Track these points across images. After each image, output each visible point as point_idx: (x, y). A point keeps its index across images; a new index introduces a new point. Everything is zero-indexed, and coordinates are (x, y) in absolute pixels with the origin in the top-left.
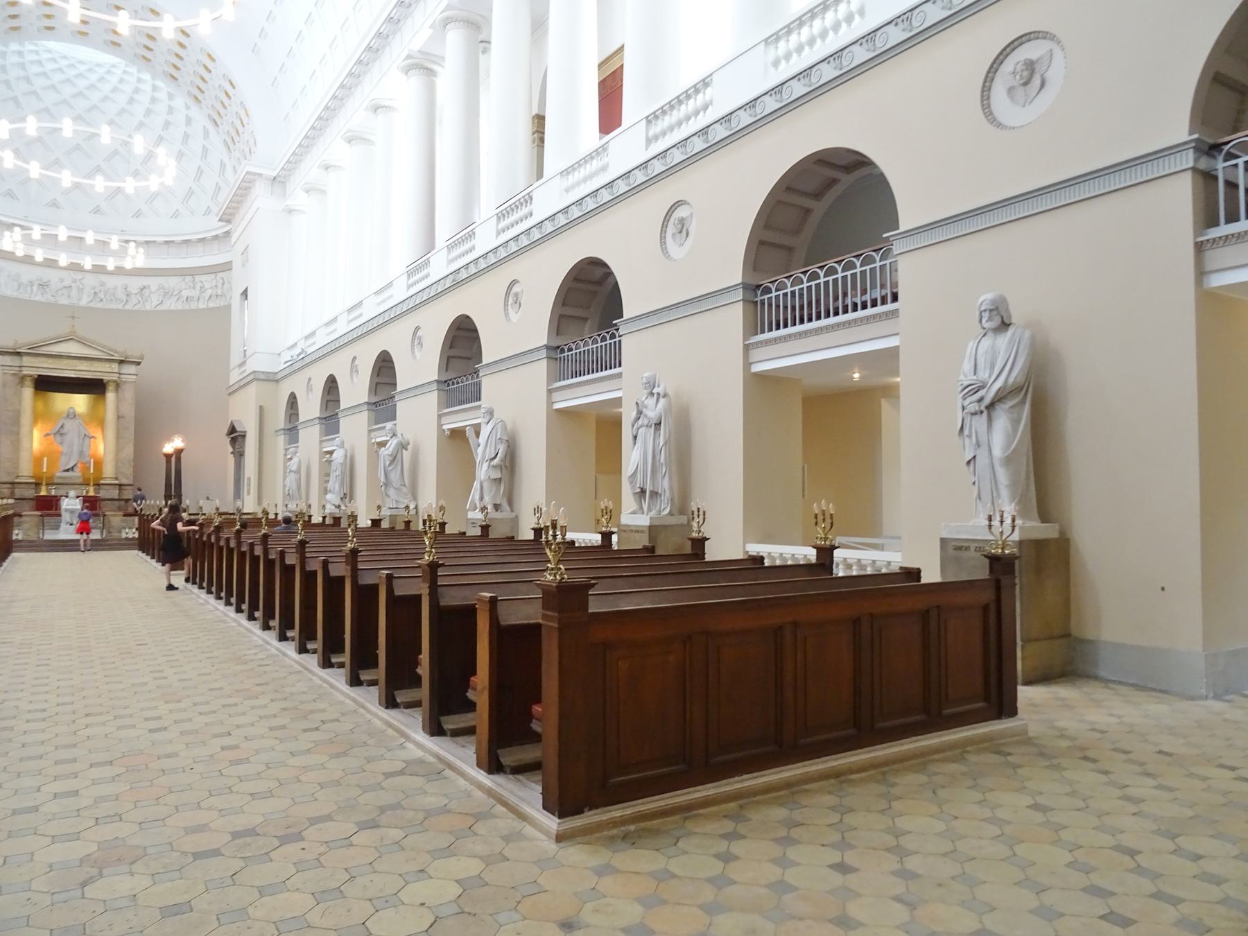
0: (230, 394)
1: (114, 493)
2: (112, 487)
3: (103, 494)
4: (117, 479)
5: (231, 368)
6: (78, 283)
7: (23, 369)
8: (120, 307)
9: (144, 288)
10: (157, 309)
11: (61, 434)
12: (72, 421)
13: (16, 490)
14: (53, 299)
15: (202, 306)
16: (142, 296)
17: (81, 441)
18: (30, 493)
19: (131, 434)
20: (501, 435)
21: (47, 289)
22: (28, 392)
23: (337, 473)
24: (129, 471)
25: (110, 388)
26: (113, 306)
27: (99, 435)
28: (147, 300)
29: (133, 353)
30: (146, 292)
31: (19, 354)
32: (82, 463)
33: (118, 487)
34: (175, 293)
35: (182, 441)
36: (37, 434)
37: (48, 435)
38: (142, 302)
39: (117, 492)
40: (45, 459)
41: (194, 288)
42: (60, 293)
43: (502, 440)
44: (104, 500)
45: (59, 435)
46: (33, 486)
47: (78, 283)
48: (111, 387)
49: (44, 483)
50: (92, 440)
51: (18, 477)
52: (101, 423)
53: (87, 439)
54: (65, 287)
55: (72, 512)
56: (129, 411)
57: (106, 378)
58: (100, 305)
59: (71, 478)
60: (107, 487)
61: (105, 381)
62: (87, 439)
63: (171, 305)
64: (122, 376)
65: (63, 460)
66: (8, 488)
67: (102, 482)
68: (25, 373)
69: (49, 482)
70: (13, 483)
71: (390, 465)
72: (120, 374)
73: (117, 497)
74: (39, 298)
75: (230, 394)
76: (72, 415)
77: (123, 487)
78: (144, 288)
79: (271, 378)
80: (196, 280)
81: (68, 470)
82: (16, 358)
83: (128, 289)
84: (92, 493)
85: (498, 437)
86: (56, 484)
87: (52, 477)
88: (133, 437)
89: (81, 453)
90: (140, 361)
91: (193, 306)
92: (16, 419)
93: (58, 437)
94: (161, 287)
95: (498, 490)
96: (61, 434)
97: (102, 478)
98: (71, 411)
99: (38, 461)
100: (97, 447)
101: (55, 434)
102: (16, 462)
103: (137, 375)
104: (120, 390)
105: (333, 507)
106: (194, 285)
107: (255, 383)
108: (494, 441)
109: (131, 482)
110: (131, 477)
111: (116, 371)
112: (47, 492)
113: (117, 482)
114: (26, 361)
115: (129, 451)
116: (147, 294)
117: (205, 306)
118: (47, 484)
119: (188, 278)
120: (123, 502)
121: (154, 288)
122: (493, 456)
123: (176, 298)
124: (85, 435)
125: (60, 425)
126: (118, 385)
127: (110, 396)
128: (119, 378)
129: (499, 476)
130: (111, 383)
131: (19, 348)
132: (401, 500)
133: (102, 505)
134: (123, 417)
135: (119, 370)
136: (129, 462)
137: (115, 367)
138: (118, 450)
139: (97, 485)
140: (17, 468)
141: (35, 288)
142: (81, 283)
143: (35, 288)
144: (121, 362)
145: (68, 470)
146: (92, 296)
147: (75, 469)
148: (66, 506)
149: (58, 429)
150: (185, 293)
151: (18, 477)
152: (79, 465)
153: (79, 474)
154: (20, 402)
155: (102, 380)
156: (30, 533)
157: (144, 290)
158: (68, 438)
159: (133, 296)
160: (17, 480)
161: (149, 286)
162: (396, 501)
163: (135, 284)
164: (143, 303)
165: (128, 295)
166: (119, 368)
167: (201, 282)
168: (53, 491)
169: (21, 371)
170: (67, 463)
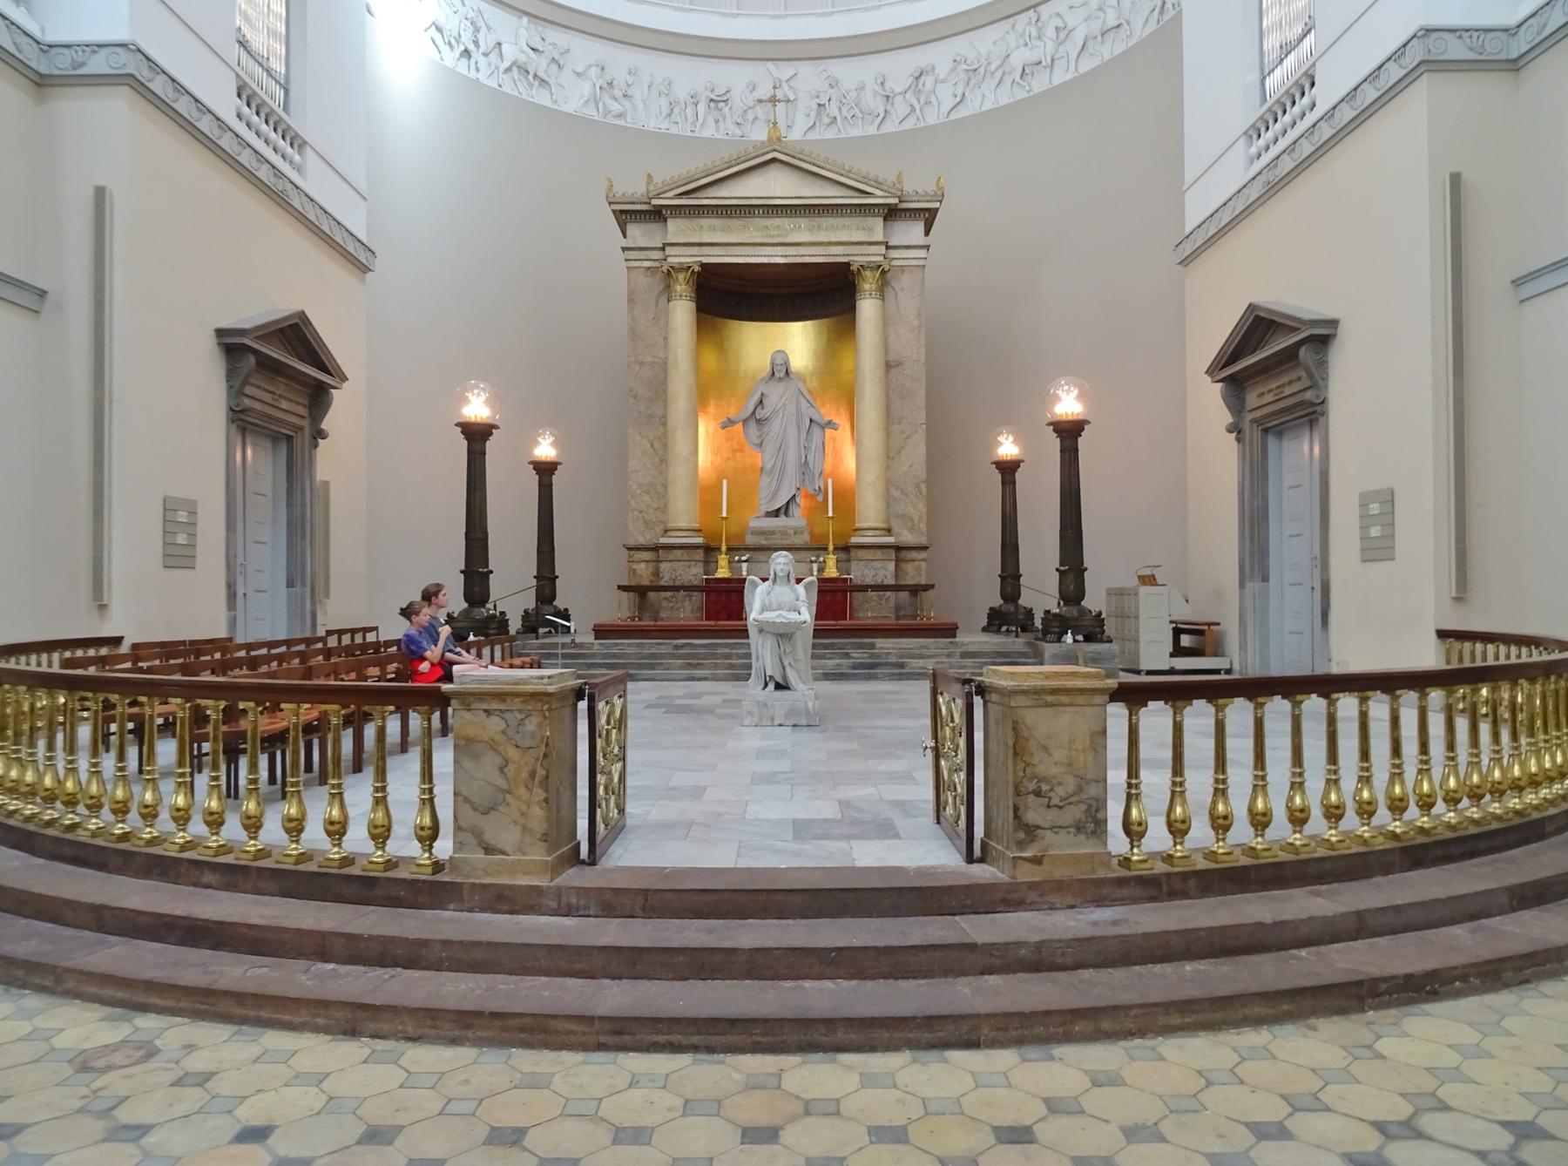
0: (1185, 262)
1: (884, 571)
2: (878, 554)
3: (861, 572)
4: (889, 531)
5: (1189, 176)
6: (785, 86)
7: (669, 250)
8: (872, 130)
9: (921, 74)
10: (954, 116)
11: (759, 421)
12: (781, 386)
13: (664, 566)
14: (738, 132)
15: (1060, 76)
16: (918, 93)
17: (803, 436)
18: (693, 573)
19: (916, 411)
21: (726, 110)
22: (683, 312)
24: (917, 509)
25: (867, 287)
26: (855, 132)
27: (842, 420)
28: (928, 103)
29: (917, 186)
30: (928, 80)
31: (657, 215)
32: (807, 496)
33: (892, 554)
34: (993, 67)
35: (1081, 397)
36: (705, 428)
37: (730, 422)
38: (918, 112)
39: (891, 566)
40: (725, 482)
41: (1039, 38)
42: (750, 116)
44: (864, 588)
45: (752, 424)
46: (700, 555)
47: (785, 86)
48: (868, 284)
49: (724, 548)
50: (828, 432)
52: (849, 398)
53: (816, 431)
54: (760, 101)
55: (783, 635)
56: (911, 348)
57: (858, 257)
58: (830, 134)
59: (784, 534)
60: (869, 554)
61: (854, 268)
62: (816, 431)
63: (985, 99)
64: (894, 254)
65: (765, 481)
66: (647, 561)
67: (854, 540)
68: (669, 260)
69: (734, 544)
70: (656, 548)
72: (888, 248)
73: (893, 582)
74: (709, 132)
75: (1185, 262)
76: (780, 371)
77: (903, 554)
78: (921, 74)
79: (1494, 48)
80: (1044, 17)
81: (776, 513)
82: (654, 227)
83: (888, 85)
84: (832, 572)
86: (748, 549)
87: (742, 536)
88: (922, 417)
90: (937, 205)
91: (1039, 83)
92: (659, 391)
93: (753, 429)
96: (759, 421)
98: (779, 361)
99: (708, 496)
100: (838, 456)
101: (745, 421)
102: (660, 490)
103: (927, 247)
104: (889, 293)
106: (1040, 30)
107: (1424, 81)
109: (923, 541)
110: (923, 526)
111: (879, 237)
112: (731, 569)
113: (890, 540)
114: (676, 229)
115: (916, 453)
116: (929, 86)
117: (1069, 76)
118: (729, 550)
119: (1022, 20)
120: (904, 595)
121: (942, 71)
123: (1000, 73)
124: (811, 420)
125: (758, 395)
126: (884, 276)
127: (867, 308)
130: (868, 273)
131: (657, 196)
133: (855, 603)
134: (899, 364)
135: (885, 236)
136: (918, 486)
137: (876, 228)
138: (890, 456)
139: (845, 549)
140: (664, 509)
141: (702, 108)
143: (702, 108)
144: (892, 213)
145: (776, 513)
146: (813, 114)
147: (793, 510)
148: (763, 610)
149: (751, 408)
150: (1019, 58)
152: (798, 500)
153: (803, 523)
154: (666, 339)
155: (848, 264)
156: (504, 833)
157: (923, 78)
158: (775, 427)
159: (899, 99)
160: (664, 540)
161: (933, 68)
163: (899, 67)
164: (921, 110)
165: (888, 97)
167: (1058, 15)
168: (744, 565)
170: (773, 497)
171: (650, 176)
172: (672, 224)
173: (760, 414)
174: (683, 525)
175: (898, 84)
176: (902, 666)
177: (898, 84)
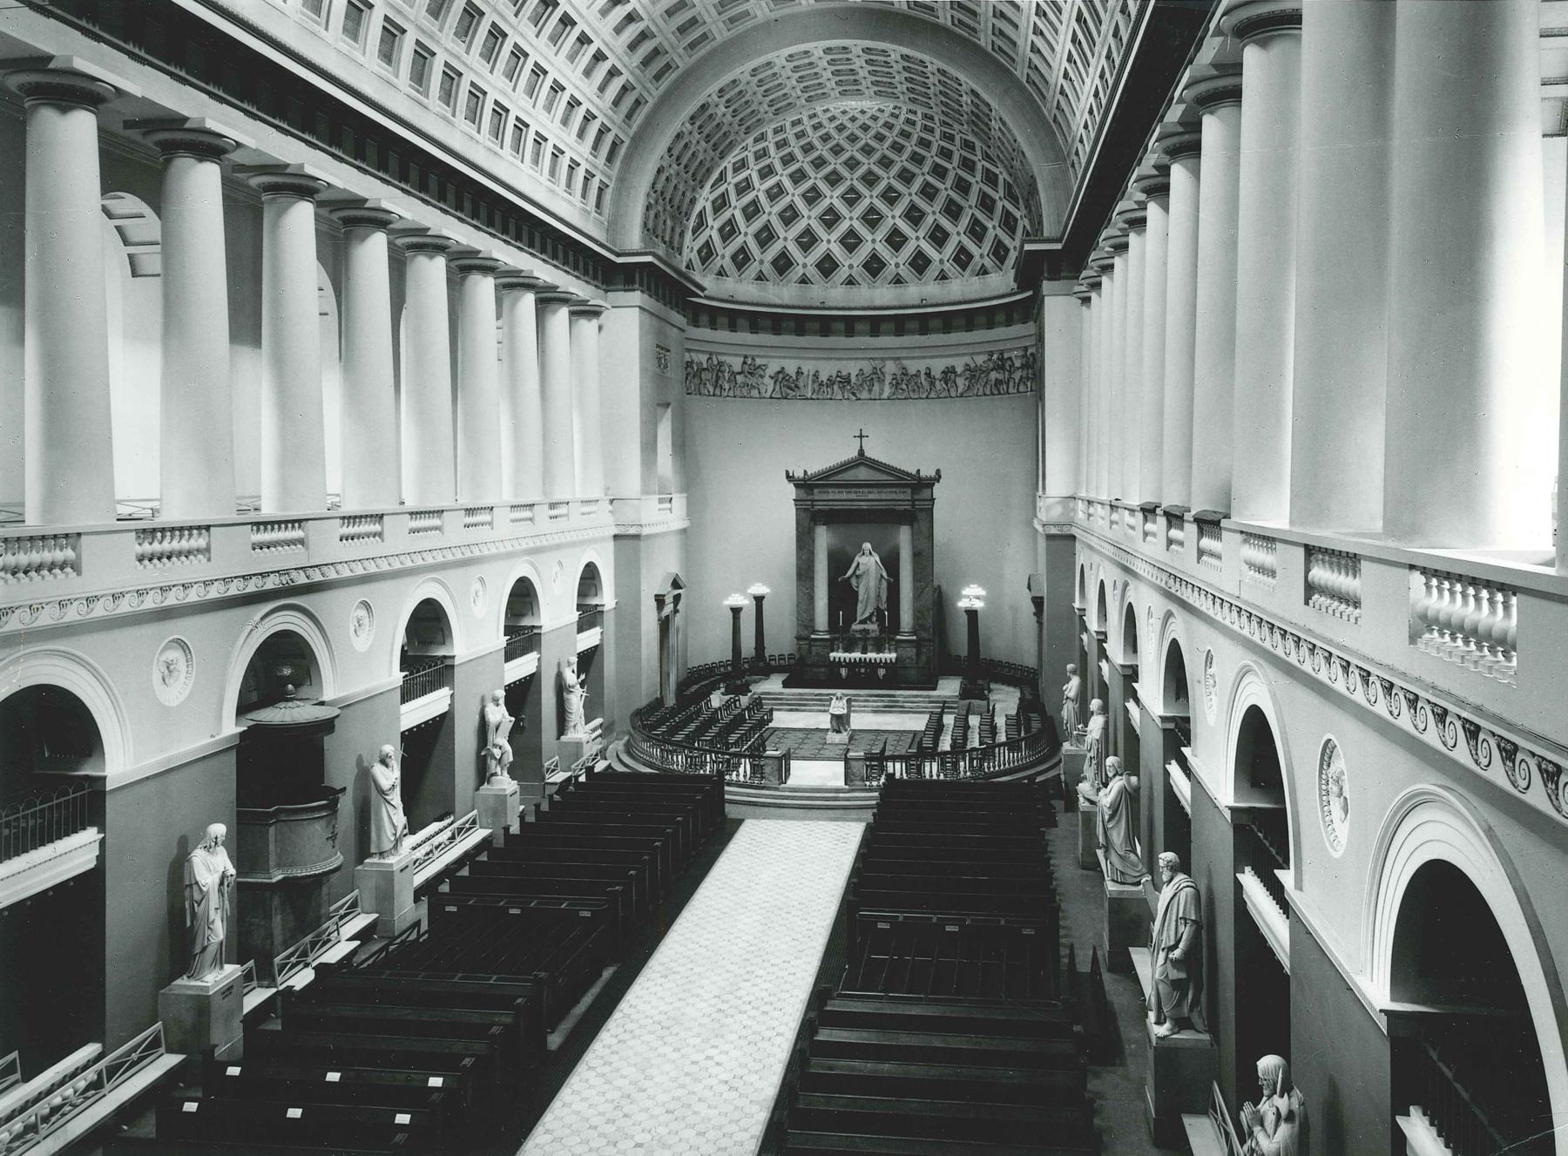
13: (813, 648)
20: (1184, 913)
23: (1092, 754)
39: (914, 650)
43: (1186, 919)
51: (814, 632)
60: (903, 645)
65: (859, 606)
71: (1109, 820)
85: (1181, 915)
89: (878, 597)
94: (967, 368)
95: (1184, 996)
96: (857, 577)
97: (898, 633)
105: (1087, 804)
108: (1173, 923)
111: (910, 498)
114: (817, 494)
121: (959, 370)
122: (1172, 943)
128: (913, 506)
129: (1183, 975)
132: (1129, 871)
142: (882, 373)
151: (814, 632)
159: (937, 382)
162: (1122, 873)
166: (912, 494)
169: (813, 505)
171: (805, 472)
172: (816, 491)
173: (858, 573)
174: (821, 629)
175: (937, 373)
176: (903, 707)
177: (937, 373)
